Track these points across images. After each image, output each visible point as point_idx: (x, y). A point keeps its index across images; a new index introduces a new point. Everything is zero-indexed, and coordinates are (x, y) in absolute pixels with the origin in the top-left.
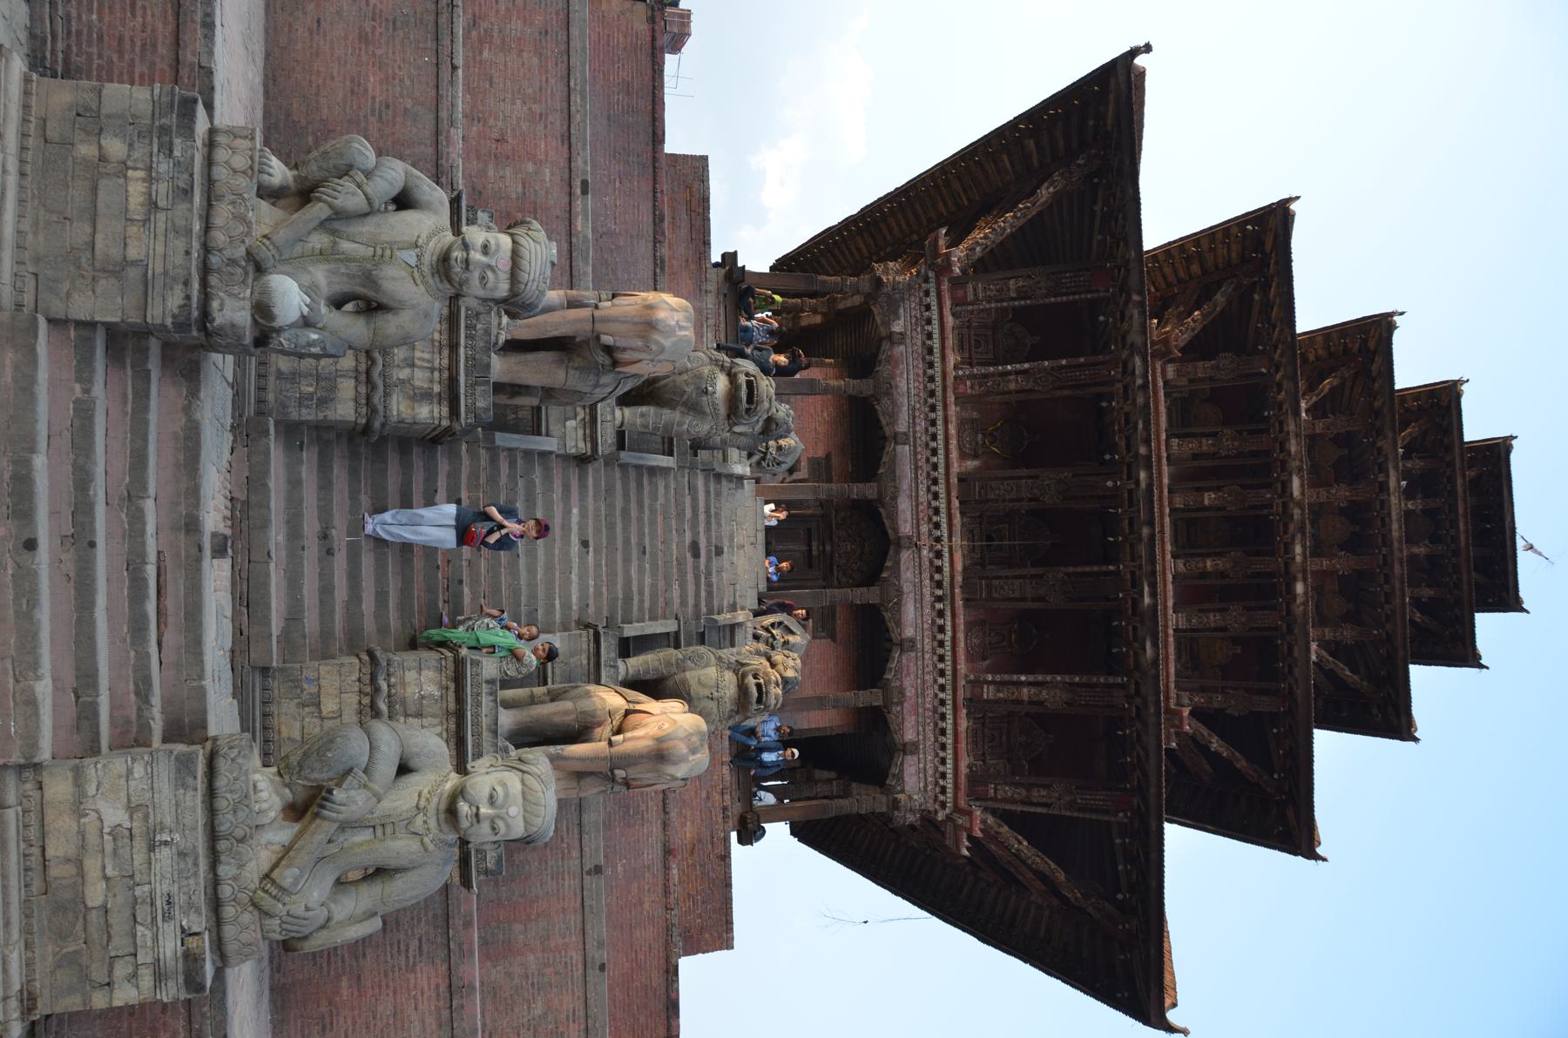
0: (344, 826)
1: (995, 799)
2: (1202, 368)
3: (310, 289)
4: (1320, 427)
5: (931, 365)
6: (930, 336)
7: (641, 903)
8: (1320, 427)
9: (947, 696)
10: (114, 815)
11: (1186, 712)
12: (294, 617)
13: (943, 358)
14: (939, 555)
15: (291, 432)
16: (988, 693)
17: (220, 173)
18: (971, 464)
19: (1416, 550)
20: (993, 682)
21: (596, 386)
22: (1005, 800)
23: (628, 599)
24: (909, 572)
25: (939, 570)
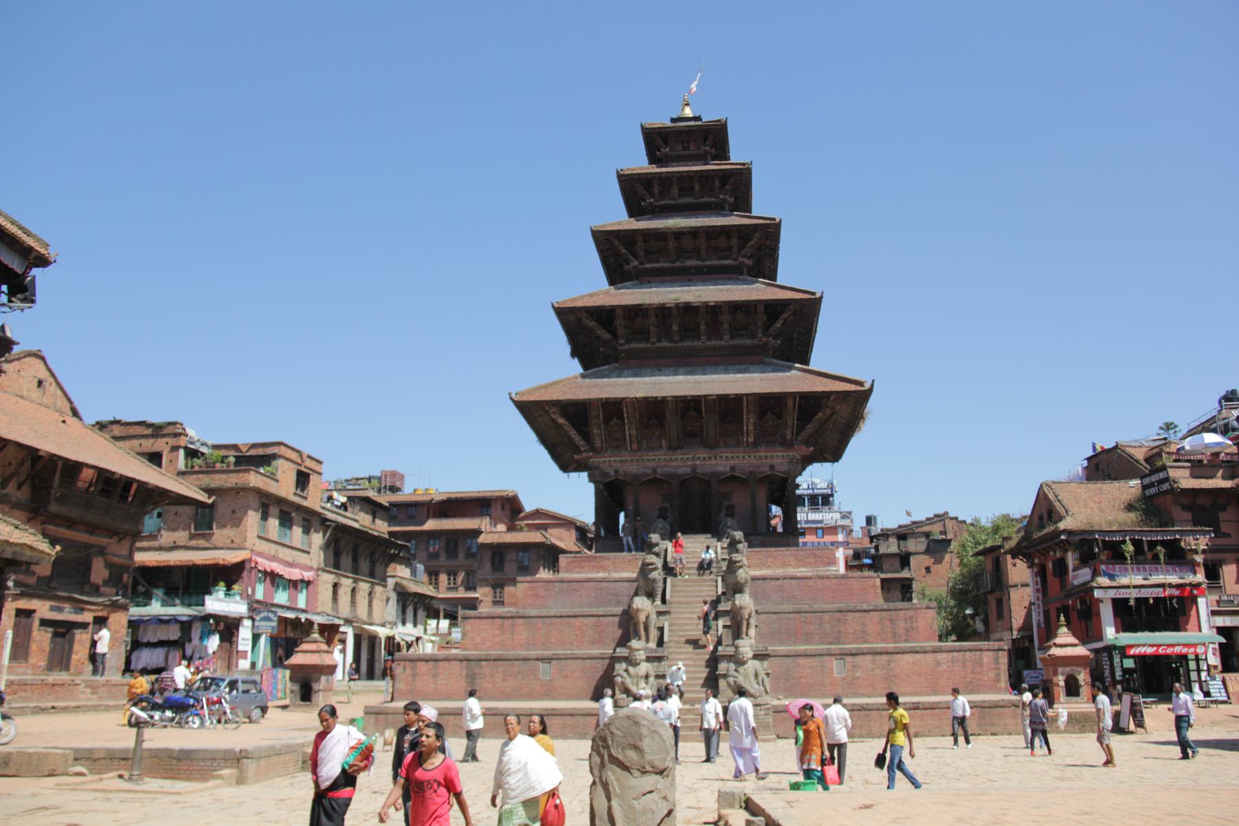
4: (642, 253)
16: (751, 439)
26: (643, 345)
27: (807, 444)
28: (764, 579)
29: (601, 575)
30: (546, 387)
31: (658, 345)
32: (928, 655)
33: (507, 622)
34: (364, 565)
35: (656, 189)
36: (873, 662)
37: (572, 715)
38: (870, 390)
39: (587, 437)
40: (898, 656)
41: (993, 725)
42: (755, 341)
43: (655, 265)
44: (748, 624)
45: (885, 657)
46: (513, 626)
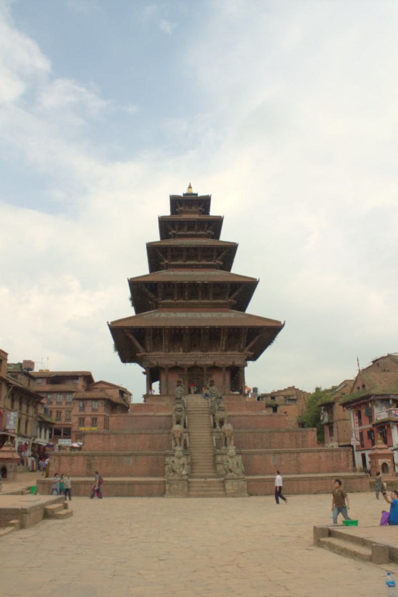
0: (233, 467)
3: (183, 471)
4: (169, 257)
5: (162, 358)
6: (157, 358)
9: (224, 356)
10: (230, 487)
11: (230, 300)
12: (212, 472)
13: (161, 355)
15: (192, 472)
16: (224, 348)
18: (181, 349)
23: (207, 425)
24: (201, 362)
25: (201, 357)
26: (170, 301)
27: (250, 350)
29: (151, 414)
31: (177, 301)
33: (107, 436)
35: (177, 227)
38: (283, 326)
39: (143, 345)
42: (225, 301)
44: (231, 439)
45: (295, 455)
46: (109, 438)
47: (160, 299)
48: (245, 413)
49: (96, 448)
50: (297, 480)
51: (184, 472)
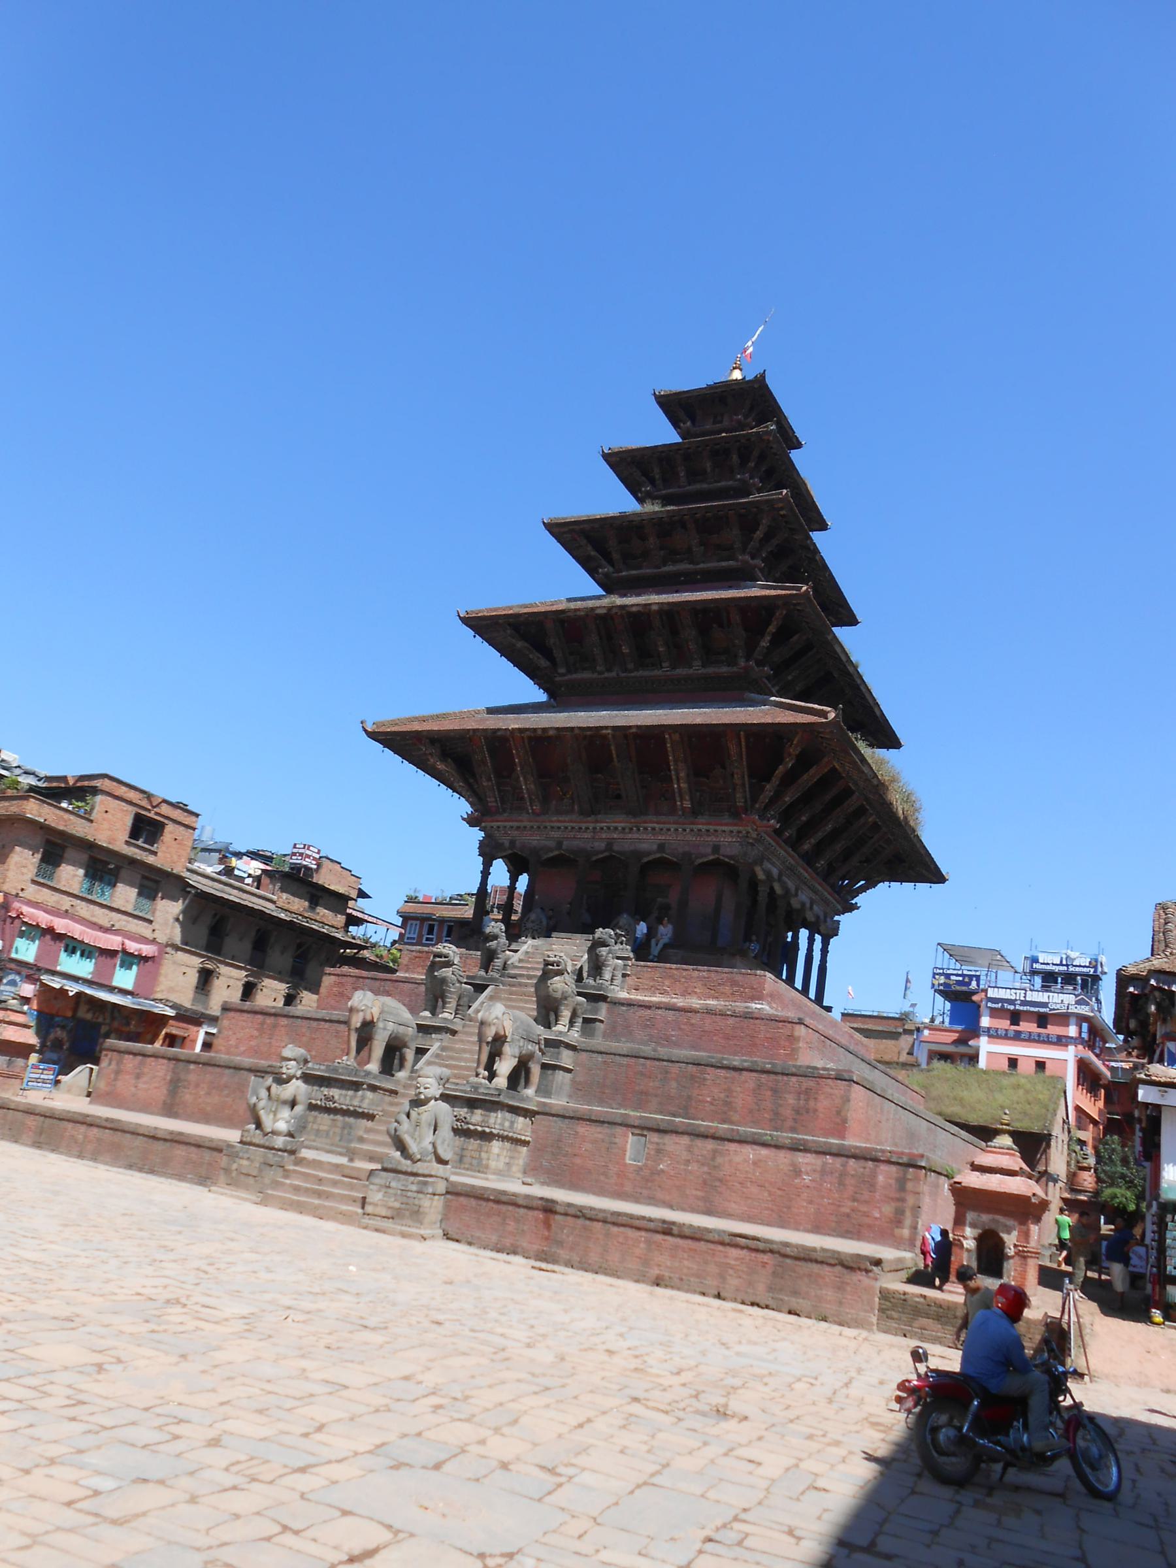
1: (746, 802)
2: (558, 654)
7: (692, 1025)
8: (616, 556)
9: (688, 828)
10: (380, 1196)
14: (616, 828)
16: (687, 804)
17: (248, 1139)
19: (709, 470)
20: (681, 801)
21: (385, 1029)
22: (745, 798)
25: (624, 829)
26: (586, 675)
28: (630, 1004)
30: (424, 719)
31: (606, 675)
32: (782, 1154)
33: (270, 1020)
34: (280, 957)
35: (657, 473)
36: (689, 1149)
37: (199, 1146)
40: (733, 1147)
41: (795, 1293)
42: (735, 669)
43: (634, 572)
45: (710, 1145)
46: (275, 1026)
47: (562, 670)
48: (695, 1002)
49: (242, 1049)
50: (605, 1221)
51: (282, 1126)
